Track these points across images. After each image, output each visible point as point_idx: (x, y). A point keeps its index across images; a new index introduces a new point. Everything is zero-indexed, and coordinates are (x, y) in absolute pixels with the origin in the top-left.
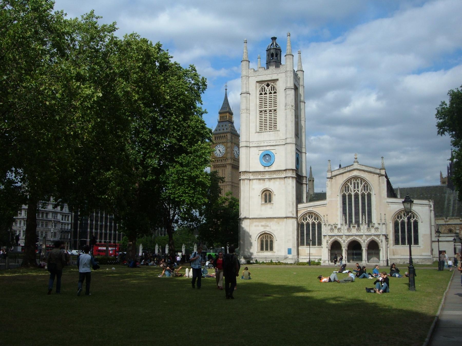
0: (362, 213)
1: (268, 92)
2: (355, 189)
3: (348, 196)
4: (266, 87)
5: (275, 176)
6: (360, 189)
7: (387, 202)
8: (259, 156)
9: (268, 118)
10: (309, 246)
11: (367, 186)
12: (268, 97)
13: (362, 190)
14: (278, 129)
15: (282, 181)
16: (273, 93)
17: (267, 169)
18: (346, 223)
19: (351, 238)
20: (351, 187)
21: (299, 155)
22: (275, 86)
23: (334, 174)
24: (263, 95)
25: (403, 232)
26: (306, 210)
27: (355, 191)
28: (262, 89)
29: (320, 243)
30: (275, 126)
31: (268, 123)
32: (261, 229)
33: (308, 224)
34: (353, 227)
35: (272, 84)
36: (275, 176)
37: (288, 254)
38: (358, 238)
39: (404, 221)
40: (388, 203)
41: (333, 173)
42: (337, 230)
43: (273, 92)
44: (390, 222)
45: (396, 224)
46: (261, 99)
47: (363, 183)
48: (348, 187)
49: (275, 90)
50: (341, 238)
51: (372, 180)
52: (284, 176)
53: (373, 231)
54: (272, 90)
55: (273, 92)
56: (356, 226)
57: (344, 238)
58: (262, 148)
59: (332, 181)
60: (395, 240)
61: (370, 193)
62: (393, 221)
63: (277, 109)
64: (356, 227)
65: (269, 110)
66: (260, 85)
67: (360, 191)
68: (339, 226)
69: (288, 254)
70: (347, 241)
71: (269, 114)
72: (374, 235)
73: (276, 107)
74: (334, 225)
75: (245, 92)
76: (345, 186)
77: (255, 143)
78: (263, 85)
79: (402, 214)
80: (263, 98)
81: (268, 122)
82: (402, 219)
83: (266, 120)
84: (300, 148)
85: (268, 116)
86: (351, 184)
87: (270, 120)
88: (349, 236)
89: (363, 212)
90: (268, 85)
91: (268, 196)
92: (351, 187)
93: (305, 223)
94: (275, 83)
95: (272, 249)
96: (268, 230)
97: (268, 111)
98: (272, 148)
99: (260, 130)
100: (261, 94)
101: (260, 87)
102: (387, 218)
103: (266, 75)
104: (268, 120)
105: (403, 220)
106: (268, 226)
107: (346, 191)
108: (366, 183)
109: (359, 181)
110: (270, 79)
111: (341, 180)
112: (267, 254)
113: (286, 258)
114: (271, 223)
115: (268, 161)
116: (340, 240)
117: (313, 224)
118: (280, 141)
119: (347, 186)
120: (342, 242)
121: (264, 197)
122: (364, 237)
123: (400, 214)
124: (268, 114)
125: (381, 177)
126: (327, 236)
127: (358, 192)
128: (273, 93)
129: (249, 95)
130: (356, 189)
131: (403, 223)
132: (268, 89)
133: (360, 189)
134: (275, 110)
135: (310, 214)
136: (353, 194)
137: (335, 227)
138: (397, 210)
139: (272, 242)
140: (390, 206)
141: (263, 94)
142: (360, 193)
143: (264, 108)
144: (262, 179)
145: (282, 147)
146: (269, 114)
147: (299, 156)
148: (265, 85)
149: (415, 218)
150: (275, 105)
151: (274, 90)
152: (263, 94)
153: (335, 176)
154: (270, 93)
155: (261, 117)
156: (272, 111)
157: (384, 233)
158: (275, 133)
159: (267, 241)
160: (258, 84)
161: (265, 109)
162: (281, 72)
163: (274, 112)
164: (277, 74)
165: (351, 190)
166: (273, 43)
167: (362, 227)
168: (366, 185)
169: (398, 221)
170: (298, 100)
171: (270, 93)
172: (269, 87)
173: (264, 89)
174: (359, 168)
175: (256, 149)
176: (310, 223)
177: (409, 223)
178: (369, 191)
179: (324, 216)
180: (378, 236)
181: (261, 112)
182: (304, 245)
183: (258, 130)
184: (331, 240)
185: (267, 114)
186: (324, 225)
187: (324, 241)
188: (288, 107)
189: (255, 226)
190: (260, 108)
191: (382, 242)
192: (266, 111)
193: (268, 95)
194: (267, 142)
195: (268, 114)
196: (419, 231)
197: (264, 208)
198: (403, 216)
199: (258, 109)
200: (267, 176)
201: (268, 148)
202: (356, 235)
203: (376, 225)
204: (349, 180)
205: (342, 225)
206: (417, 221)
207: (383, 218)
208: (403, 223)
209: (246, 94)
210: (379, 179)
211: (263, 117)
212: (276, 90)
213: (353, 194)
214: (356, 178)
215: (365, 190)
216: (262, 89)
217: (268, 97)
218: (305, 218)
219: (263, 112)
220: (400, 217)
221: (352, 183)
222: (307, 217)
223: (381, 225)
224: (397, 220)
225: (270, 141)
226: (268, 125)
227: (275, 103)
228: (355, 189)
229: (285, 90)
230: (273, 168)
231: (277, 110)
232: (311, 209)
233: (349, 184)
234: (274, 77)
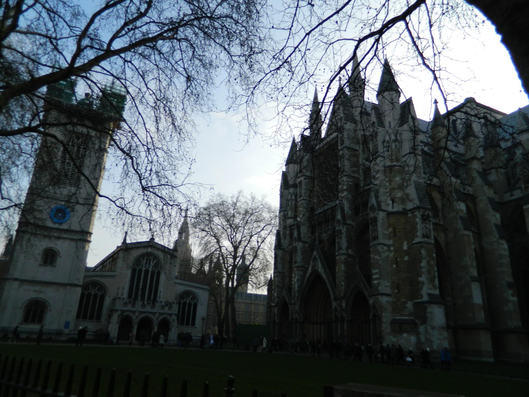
5: (65, 236)
15: (73, 244)
17: (56, 226)
19: (144, 315)
23: (129, 246)
26: (90, 279)
27: (145, 267)
32: (33, 295)
33: (89, 294)
36: (65, 236)
38: (150, 315)
47: (155, 261)
48: (140, 262)
50: (134, 314)
52: (77, 238)
57: (137, 314)
64: (151, 304)
67: (151, 267)
76: (138, 261)
79: (185, 295)
86: (143, 260)
88: (142, 313)
96: (42, 296)
108: (157, 261)
111: (135, 254)
113: (59, 333)
116: (133, 316)
120: (134, 318)
122: (157, 315)
130: (147, 265)
131: (185, 303)
135: (95, 284)
136: (144, 269)
138: (182, 291)
142: (150, 269)
176: (93, 294)
177: (190, 305)
178: (159, 269)
180: (171, 315)
191: (174, 321)
196: (197, 313)
200: (56, 234)
202: (150, 313)
204: (143, 256)
208: (185, 303)
213: (144, 269)
215: (155, 268)
221: (145, 258)
222: (91, 287)
223: (175, 304)
230: (65, 226)
232: (97, 279)
233: (142, 259)
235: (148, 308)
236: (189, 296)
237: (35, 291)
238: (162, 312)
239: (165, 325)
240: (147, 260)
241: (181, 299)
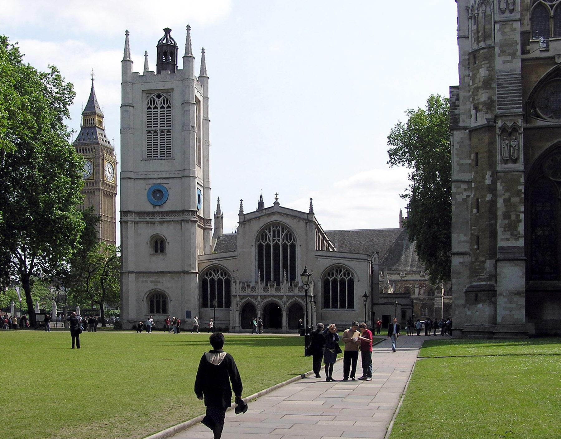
0: (284, 268)
1: (159, 106)
2: (274, 238)
3: (265, 246)
4: (156, 99)
7: (315, 255)
8: (147, 191)
9: (159, 141)
10: (213, 308)
11: (290, 235)
12: (159, 113)
16: (166, 108)
18: (262, 280)
20: (269, 236)
21: (201, 191)
23: (247, 218)
27: (274, 240)
30: (168, 153)
31: (159, 148)
35: (165, 95)
39: (337, 279)
40: (316, 257)
41: (245, 216)
43: (165, 106)
44: (319, 280)
45: (326, 283)
46: (149, 115)
49: (169, 103)
51: (297, 228)
54: (164, 104)
55: (165, 106)
56: (275, 285)
58: (150, 182)
59: (244, 227)
60: (325, 303)
61: (294, 244)
62: (322, 281)
63: (171, 130)
65: (160, 130)
66: (148, 95)
71: (161, 135)
73: (170, 126)
75: (127, 104)
76: (262, 235)
77: (141, 173)
78: (152, 96)
80: (152, 113)
82: (335, 276)
83: (156, 144)
84: (203, 182)
85: (159, 139)
86: (270, 232)
87: (162, 144)
89: (285, 266)
90: (159, 96)
91: (159, 245)
92: (270, 235)
94: (169, 94)
97: (159, 132)
99: (148, 157)
101: (147, 98)
103: (156, 83)
104: (159, 144)
108: (288, 232)
109: (279, 227)
111: (256, 227)
118: (176, 172)
119: (264, 234)
123: (331, 271)
124: (159, 136)
125: (309, 224)
127: (279, 241)
128: (166, 108)
129: (132, 108)
130: (276, 238)
131: (335, 281)
132: (159, 102)
134: (169, 131)
136: (272, 244)
138: (328, 265)
140: (319, 261)
141: (152, 109)
142: (281, 243)
143: (154, 127)
145: (178, 180)
146: (161, 135)
147: (201, 193)
148: (154, 96)
149: (350, 276)
150: (169, 125)
151: (167, 104)
152: (152, 109)
153: (249, 221)
154: (162, 107)
155: (149, 139)
156: (164, 132)
158: (169, 161)
160: (144, 94)
161: (154, 129)
162: (177, 79)
163: (167, 134)
164: (171, 82)
165: (269, 240)
167: (282, 286)
168: (289, 234)
169: (329, 279)
170: (200, 116)
171: (162, 107)
172: (161, 98)
174: (280, 211)
177: (343, 282)
178: (292, 240)
179: (234, 271)
181: (149, 132)
183: (145, 156)
185: (157, 135)
186: (234, 282)
187: (234, 305)
188: (187, 128)
190: (148, 127)
192: (155, 132)
193: (159, 108)
194: (158, 173)
195: (159, 136)
198: (335, 272)
199: (144, 129)
201: (159, 181)
204: (267, 227)
206: (353, 279)
208: (335, 281)
209: (128, 107)
210: (306, 227)
212: (170, 103)
213: (272, 244)
214: (276, 224)
217: (159, 113)
219: (152, 132)
220: (331, 274)
224: (327, 278)
225: (162, 173)
226: (159, 151)
227: (169, 120)
228: (274, 238)
229: (183, 105)
231: (171, 132)
233: (267, 232)
234: (168, 86)
236: (341, 271)
241: (329, 275)
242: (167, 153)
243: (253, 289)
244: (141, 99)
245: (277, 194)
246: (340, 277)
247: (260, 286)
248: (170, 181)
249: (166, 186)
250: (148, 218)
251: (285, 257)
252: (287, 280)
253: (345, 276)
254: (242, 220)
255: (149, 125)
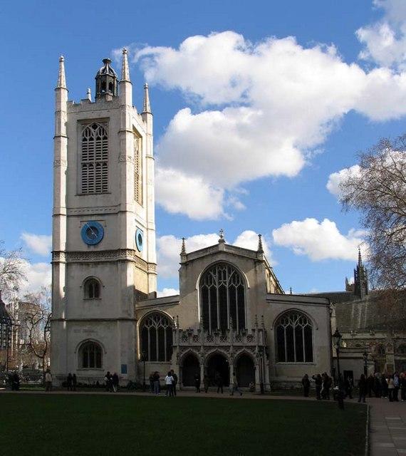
1: (94, 137)
4: (92, 130)
5: (103, 259)
6: (228, 280)
11: (238, 278)
12: (95, 144)
13: (230, 283)
14: (109, 190)
15: (114, 267)
17: (92, 249)
19: (212, 351)
22: (105, 128)
24: (88, 142)
25: (290, 342)
27: (219, 283)
28: (86, 131)
29: (169, 358)
31: (94, 183)
32: (83, 336)
33: (153, 330)
34: (216, 334)
36: (103, 259)
37: (122, 373)
42: (191, 339)
43: (101, 137)
45: (279, 332)
48: (211, 276)
53: (245, 341)
55: (101, 137)
57: (202, 350)
58: (85, 219)
68: (196, 333)
69: (122, 373)
70: (206, 355)
72: (246, 347)
74: (188, 330)
76: (206, 278)
81: (95, 180)
88: (210, 347)
90: (95, 127)
92: (216, 277)
93: (149, 328)
95: (99, 365)
96: (93, 337)
97: (94, 165)
98: (100, 218)
100: (85, 140)
102: (266, 323)
105: (289, 326)
106: (93, 332)
107: (207, 283)
108: (235, 273)
110: (98, 117)
111: (200, 269)
112: (92, 373)
114: (98, 328)
115: (94, 238)
116: (197, 353)
117: (161, 330)
120: (200, 355)
121: (88, 289)
122: (231, 350)
126: (178, 347)
131: (290, 329)
133: (228, 280)
134: (105, 164)
137: (190, 334)
139: (99, 355)
142: (227, 286)
144: (85, 262)
154: (98, 139)
157: (261, 344)
159: (92, 354)
166: (106, 68)
171: (98, 139)
173: (90, 131)
175: (76, 218)
177: (298, 330)
180: (252, 348)
181: (84, 165)
182: (147, 360)
183: (80, 192)
184: (184, 353)
189: (75, 331)
193: (95, 141)
197: (87, 304)
198: (290, 320)
200: (92, 260)
201: (93, 218)
203: (250, 332)
204: (211, 268)
205: (199, 331)
207: (260, 324)
211: (88, 173)
214: (221, 264)
216: (86, 131)
217: (95, 144)
218: (149, 321)
227: (105, 152)
230: (101, 248)
233: (212, 273)
234: (104, 114)
235: (218, 341)
237: (85, 331)
238: (240, 344)
239: (245, 363)
240: (220, 273)
242: (103, 189)
243: (196, 338)
244: (75, 130)
245: (222, 231)
246: (297, 323)
247: (204, 335)
248: (106, 218)
249: (102, 223)
250: (81, 259)
251: (233, 302)
252: (234, 328)
253: (301, 323)
254: (185, 261)
255: (84, 157)
